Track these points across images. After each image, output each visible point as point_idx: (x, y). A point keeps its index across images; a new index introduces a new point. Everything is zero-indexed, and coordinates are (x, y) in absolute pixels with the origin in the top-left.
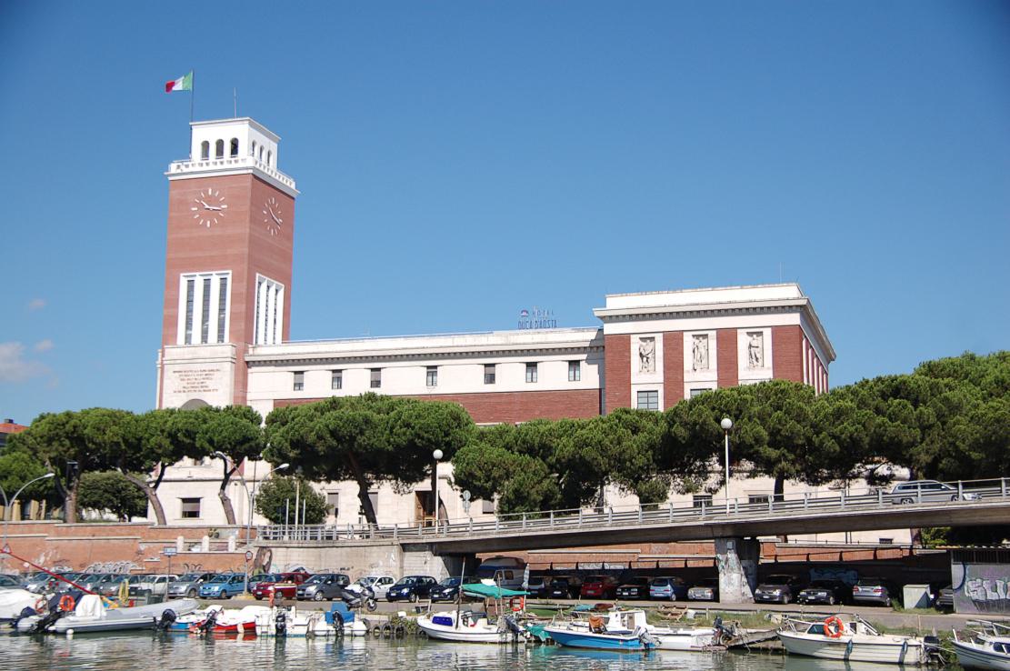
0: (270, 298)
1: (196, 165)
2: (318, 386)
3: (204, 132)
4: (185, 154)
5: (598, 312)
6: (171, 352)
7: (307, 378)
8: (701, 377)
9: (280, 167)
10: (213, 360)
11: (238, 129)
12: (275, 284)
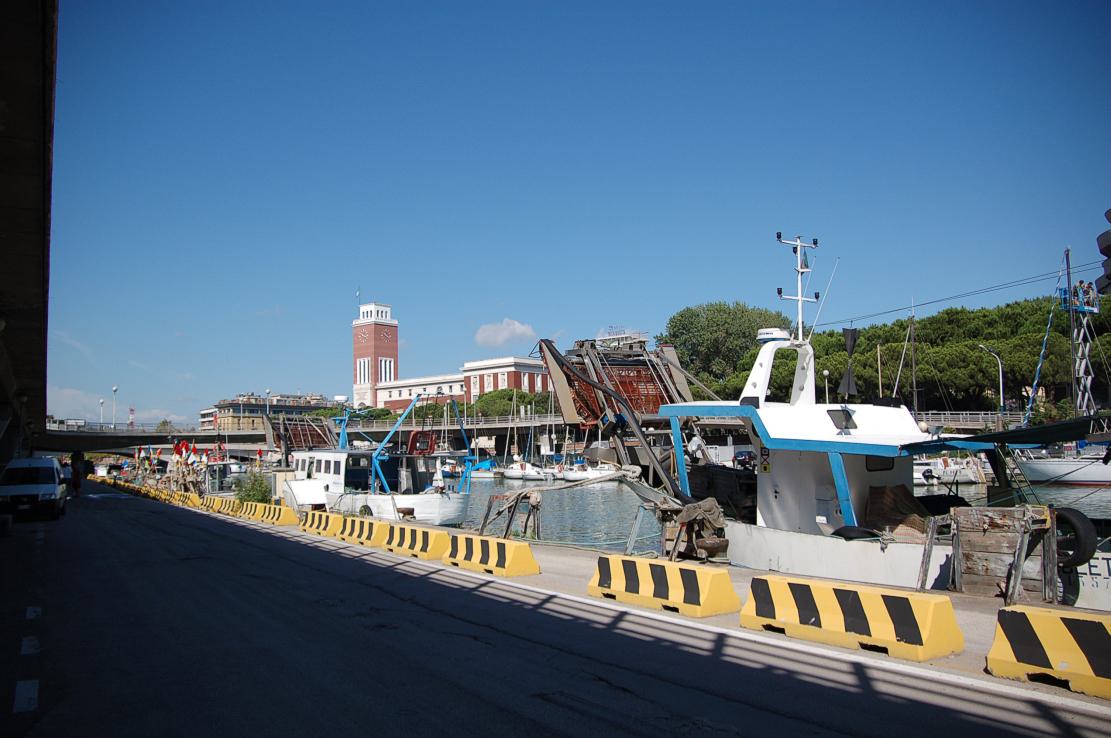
0: (387, 363)
1: (362, 321)
2: (395, 396)
3: (364, 309)
4: (358, 318)
5: (461, 369)
6: (355, 387)
7: (393, 394)
8: (489, 388)
9: (391, 317)
10: (366, 389)
11: (371, 307)
12: (388, 360)
